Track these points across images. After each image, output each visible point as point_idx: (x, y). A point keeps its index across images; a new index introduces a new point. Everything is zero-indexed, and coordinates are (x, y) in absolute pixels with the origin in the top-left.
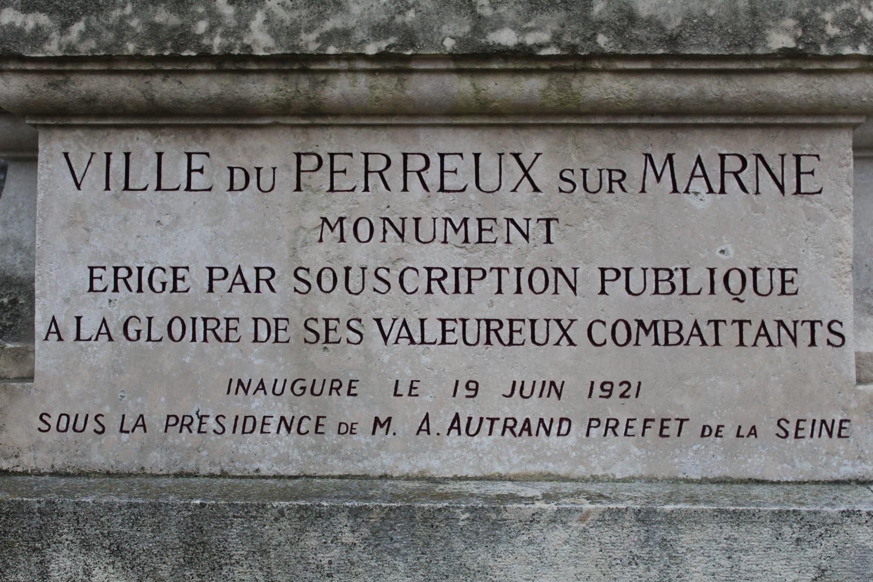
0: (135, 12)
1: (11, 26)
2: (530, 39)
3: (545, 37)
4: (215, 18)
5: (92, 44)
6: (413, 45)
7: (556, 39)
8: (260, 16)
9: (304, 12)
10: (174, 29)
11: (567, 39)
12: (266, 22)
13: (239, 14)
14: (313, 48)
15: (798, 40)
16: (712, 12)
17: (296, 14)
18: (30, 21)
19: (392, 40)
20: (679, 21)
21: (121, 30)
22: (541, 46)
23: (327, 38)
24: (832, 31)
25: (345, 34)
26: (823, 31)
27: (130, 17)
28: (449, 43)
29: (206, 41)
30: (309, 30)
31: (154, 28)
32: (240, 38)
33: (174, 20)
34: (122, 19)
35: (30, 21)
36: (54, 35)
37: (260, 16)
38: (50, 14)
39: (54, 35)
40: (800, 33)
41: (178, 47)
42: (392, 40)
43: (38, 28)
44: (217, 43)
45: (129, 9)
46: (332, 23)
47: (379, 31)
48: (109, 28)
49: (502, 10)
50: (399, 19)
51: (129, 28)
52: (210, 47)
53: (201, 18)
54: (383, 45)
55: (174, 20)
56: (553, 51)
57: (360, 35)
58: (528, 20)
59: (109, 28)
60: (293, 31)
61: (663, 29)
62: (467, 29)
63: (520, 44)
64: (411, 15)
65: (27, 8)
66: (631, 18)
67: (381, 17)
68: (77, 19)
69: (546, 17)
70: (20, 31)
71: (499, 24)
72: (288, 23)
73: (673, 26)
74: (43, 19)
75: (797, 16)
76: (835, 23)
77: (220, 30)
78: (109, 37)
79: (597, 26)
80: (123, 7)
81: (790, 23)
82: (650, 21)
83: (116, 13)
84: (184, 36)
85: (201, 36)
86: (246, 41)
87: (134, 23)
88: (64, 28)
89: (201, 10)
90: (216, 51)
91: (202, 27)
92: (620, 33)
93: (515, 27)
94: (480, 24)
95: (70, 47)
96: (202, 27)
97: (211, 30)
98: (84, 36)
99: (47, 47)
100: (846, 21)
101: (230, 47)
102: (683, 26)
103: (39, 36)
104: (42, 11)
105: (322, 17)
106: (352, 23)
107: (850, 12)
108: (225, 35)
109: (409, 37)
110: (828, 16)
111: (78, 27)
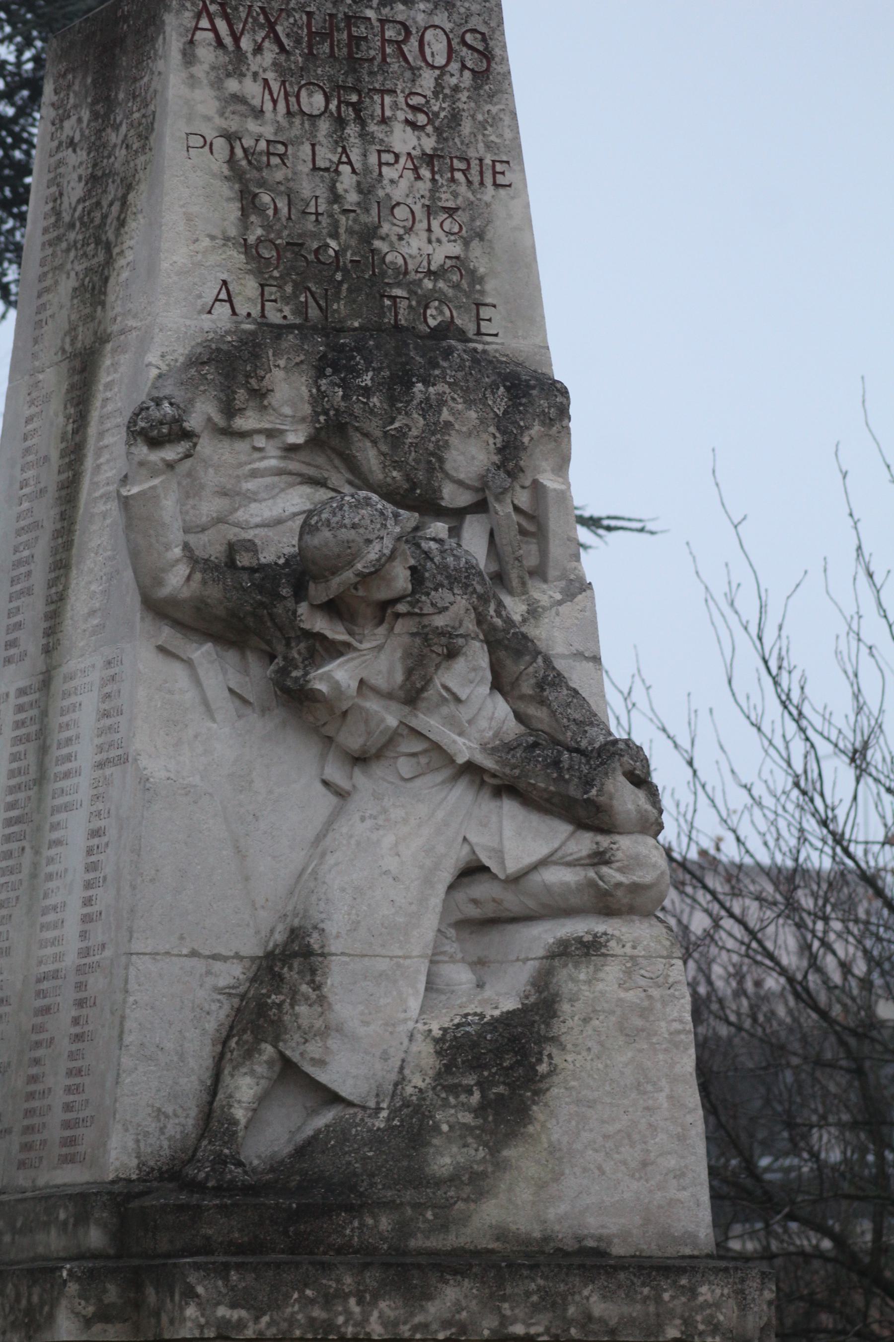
0: (300, 1310)
1: (223, 1317)
2: (533, 1331)
3: (540, 1329)
4: (348, 1313)
5: (274, 1330)
6: (465, 1334)
7: (547, 1331)
8: (376, 1314)
9: (402, 1311)
10: (324, 1321)
11: (553, 1331)
12: (379, 1317)
13: (363, 1312)
14: (407, 1335)
15: (682, 1333)
16: (634, 1314)
17: (397, 1312)
18: (235, 1315)
19: (453, 1330)
20: (616, 1320)
21: (292, 1321)
22: (539, 1335)
23: (415, 1328)
24: (701, 1327)
25: (425, 1326)
26: (696, 1327)
27: (297, 1313)
28: (486, 1333)
29: (343, 1330)
30: (405, 1323)
31: (312, 1321)
32: (364, 1328)
33: (324, 1315)
34: (293, 1314)
35: (235, 1315)
36: (251, 1324)
37: (376, 1314)
38: (248, 1310)
39: (251, 1324)
40: (683, 1328)
41: (326, 1333)
42: (453, 1330)
43: (240, 1319)
44: (350, 1331)
45: (296, 1308)
46: (418, 1319)
47: (446, 1324)
48: (285, 1320)
49: (517, 1311)
50: (457, 1317)
51: (297, 1320)
52: (346, 1333)
53: (340, 1314)
54: (448, 1333)
55: (324, 1315)
56: (545, 1338)
57: (434, 1327)
58: (531, 1318)
59: (285, 1320)
60: (396, 1324)
61: (607, 1325)
62: (496, 1323)
63: (527, 1334)
64: (464, 1314)
65: (233, 1306)
66: (590, 1318)
67: (448, 1315)
68: (264, 1314)
69: (541, 1316)
70: (229, 1322)
71: (514, 1321)
72: (392, 1318)
73: (613, 1322)
74: (243, 1313)
75: (682, 1317)
76: (702, 1323)
77: (351, 1322)
78: (284, 1325)
79: (570, 1322)
80: (293, 1306)
81: (678, 1322)
82: (601, 1320)
83: (289, 1310)
84: (329, 1326)
85: (339, 1326)
86: (367, 1330)
87: (300, 1317)
88: (257, 1319)
89: (340, 1309)
90: (349, 1336)
91: (341, 1320)
92: (583, 1327)
93: (524, 1322)
94: (504, 1321)
95: (261, 1333)
96: (341, 1320)
97: (346, 1322)
98: (269, 1325)
99: (246, 1332)
100: (708, 1321)
101: (358, 1333)
102: (618, 1323)
103: (241, 1325)
104: (243, 1308)
105: (412, 1315)
106: (430, 1319)
107: (712, 1316)
108: (354, 1325)
109: (463, 1328)
110: (699, 1318)
111: (265, 1319)
